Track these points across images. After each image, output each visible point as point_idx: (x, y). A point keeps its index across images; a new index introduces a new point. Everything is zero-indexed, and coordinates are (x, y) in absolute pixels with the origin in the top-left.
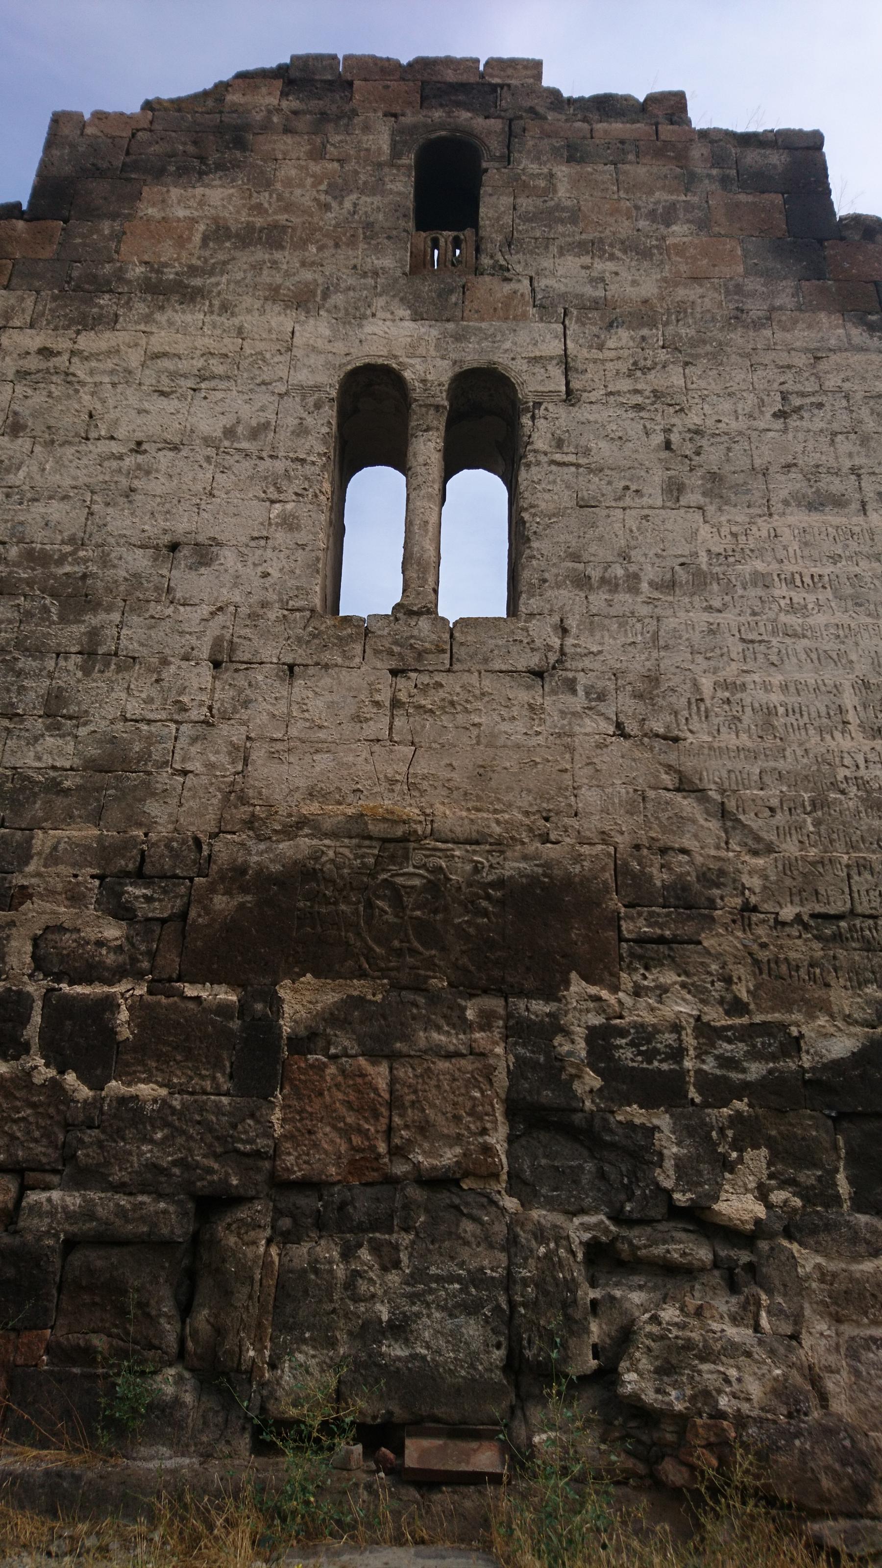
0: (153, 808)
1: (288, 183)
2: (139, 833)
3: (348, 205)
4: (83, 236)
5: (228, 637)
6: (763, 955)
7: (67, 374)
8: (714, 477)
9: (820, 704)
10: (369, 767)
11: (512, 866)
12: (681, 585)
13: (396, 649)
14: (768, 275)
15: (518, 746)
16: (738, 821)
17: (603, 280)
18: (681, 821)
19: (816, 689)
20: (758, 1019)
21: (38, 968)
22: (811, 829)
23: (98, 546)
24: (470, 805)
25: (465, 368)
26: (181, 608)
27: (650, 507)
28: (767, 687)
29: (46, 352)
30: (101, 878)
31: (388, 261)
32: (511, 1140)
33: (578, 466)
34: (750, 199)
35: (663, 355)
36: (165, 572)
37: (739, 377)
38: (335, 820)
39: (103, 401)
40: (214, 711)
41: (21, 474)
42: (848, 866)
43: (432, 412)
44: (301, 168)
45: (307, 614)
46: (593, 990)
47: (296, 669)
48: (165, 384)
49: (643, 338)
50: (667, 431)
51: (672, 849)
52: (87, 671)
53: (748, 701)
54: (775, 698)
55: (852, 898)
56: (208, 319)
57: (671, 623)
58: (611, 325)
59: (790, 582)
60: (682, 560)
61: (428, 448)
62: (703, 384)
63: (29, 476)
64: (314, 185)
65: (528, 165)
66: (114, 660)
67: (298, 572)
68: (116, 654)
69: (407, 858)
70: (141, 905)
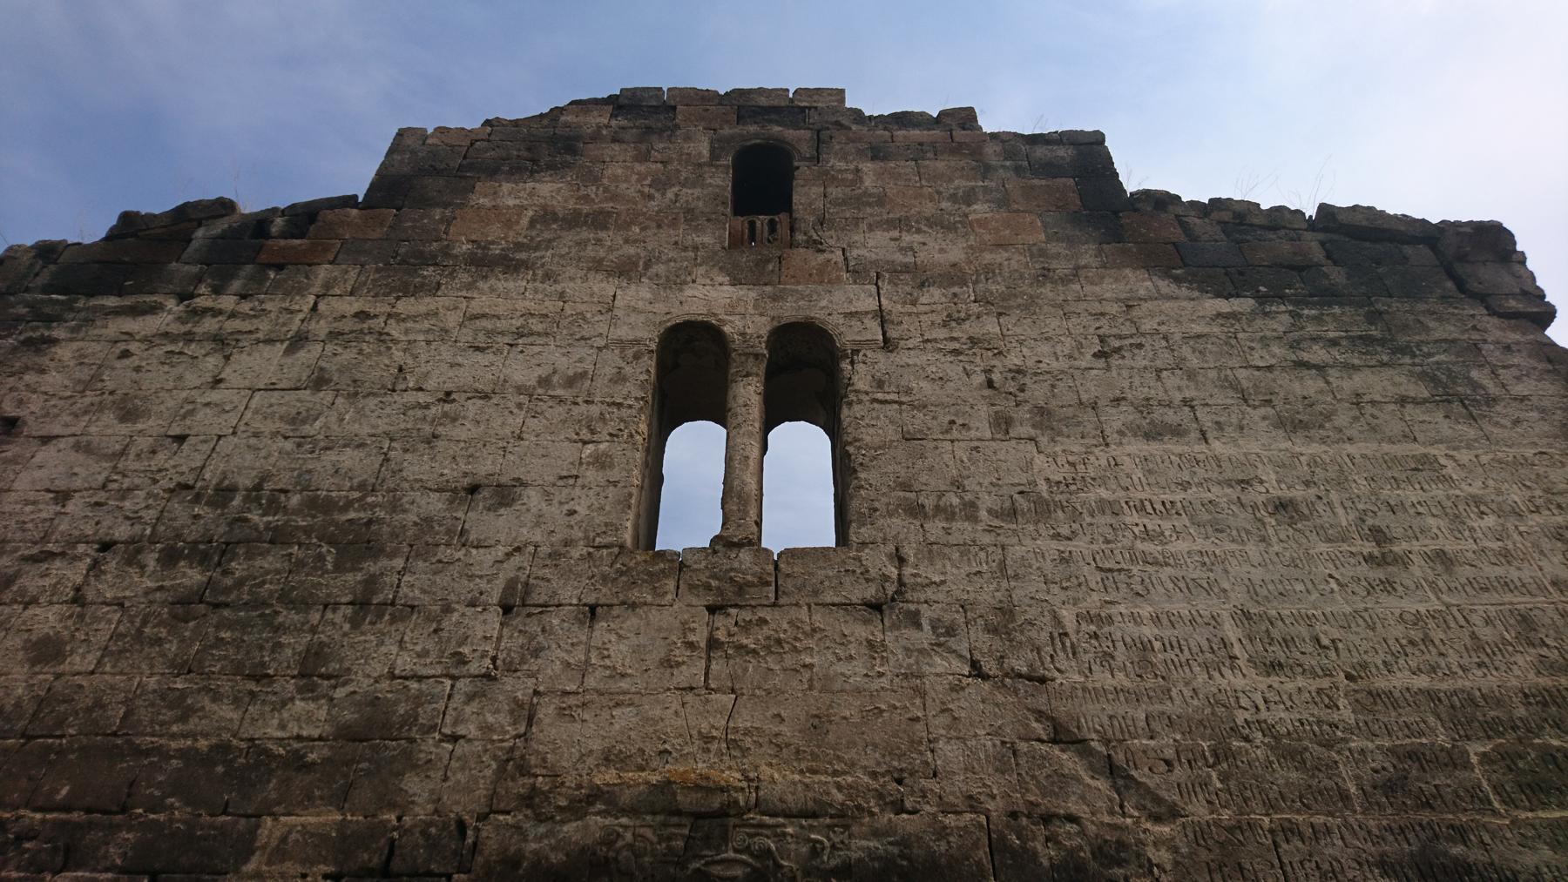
0: (413, 784)
1: (615, 178)
3: (670, 194)
4: (414, 220)
5: (523, 578)
7: (381, 334)
9: (1199, 637)
10: (680, 722)
11: (861, 846)
12: (1023, 514)
13: (714, 583)
14: (1071, 241)
15: (858, 691)
16: (1132, 778)
17: (912, 249)
18: (1062, 780)
19: (1192, 621)
22: (1219, 785)
23: (389, 491)
24: (803, 766)
26: (474, 551)
27: (979, 440)
28: (1136, 619)
29: (362, 315)
33: (900, 403)
34: (1043, 182)
35: (975, 308)
36: (460, 514)
37: (1054, 324)
38: (635, 791)
39: (415, 357)
40: (499, 662)
41: (318, 424)
42: (1272, 831)
43: (751, 359)
45: (616, 550)
47: (599, 610)
48: (481, 340)
49: (955, 295)
50: (988, 371)
51: (1057, 816)
52: (355, 623)
53: (1118, 635)
54: (1148, 631)
55: (1285, 873)
56: (530, 286)
57: (1017, 552)
58: (922, 285)
59: (1140, 508)
60: (1021, 488)
61: (748, 394)
62: (1019, 330)
63: (326, 426)
64: (638, 181)
66: (390, 609)
67: (607, 508)
68: (393, 604)
69: (725, 838)
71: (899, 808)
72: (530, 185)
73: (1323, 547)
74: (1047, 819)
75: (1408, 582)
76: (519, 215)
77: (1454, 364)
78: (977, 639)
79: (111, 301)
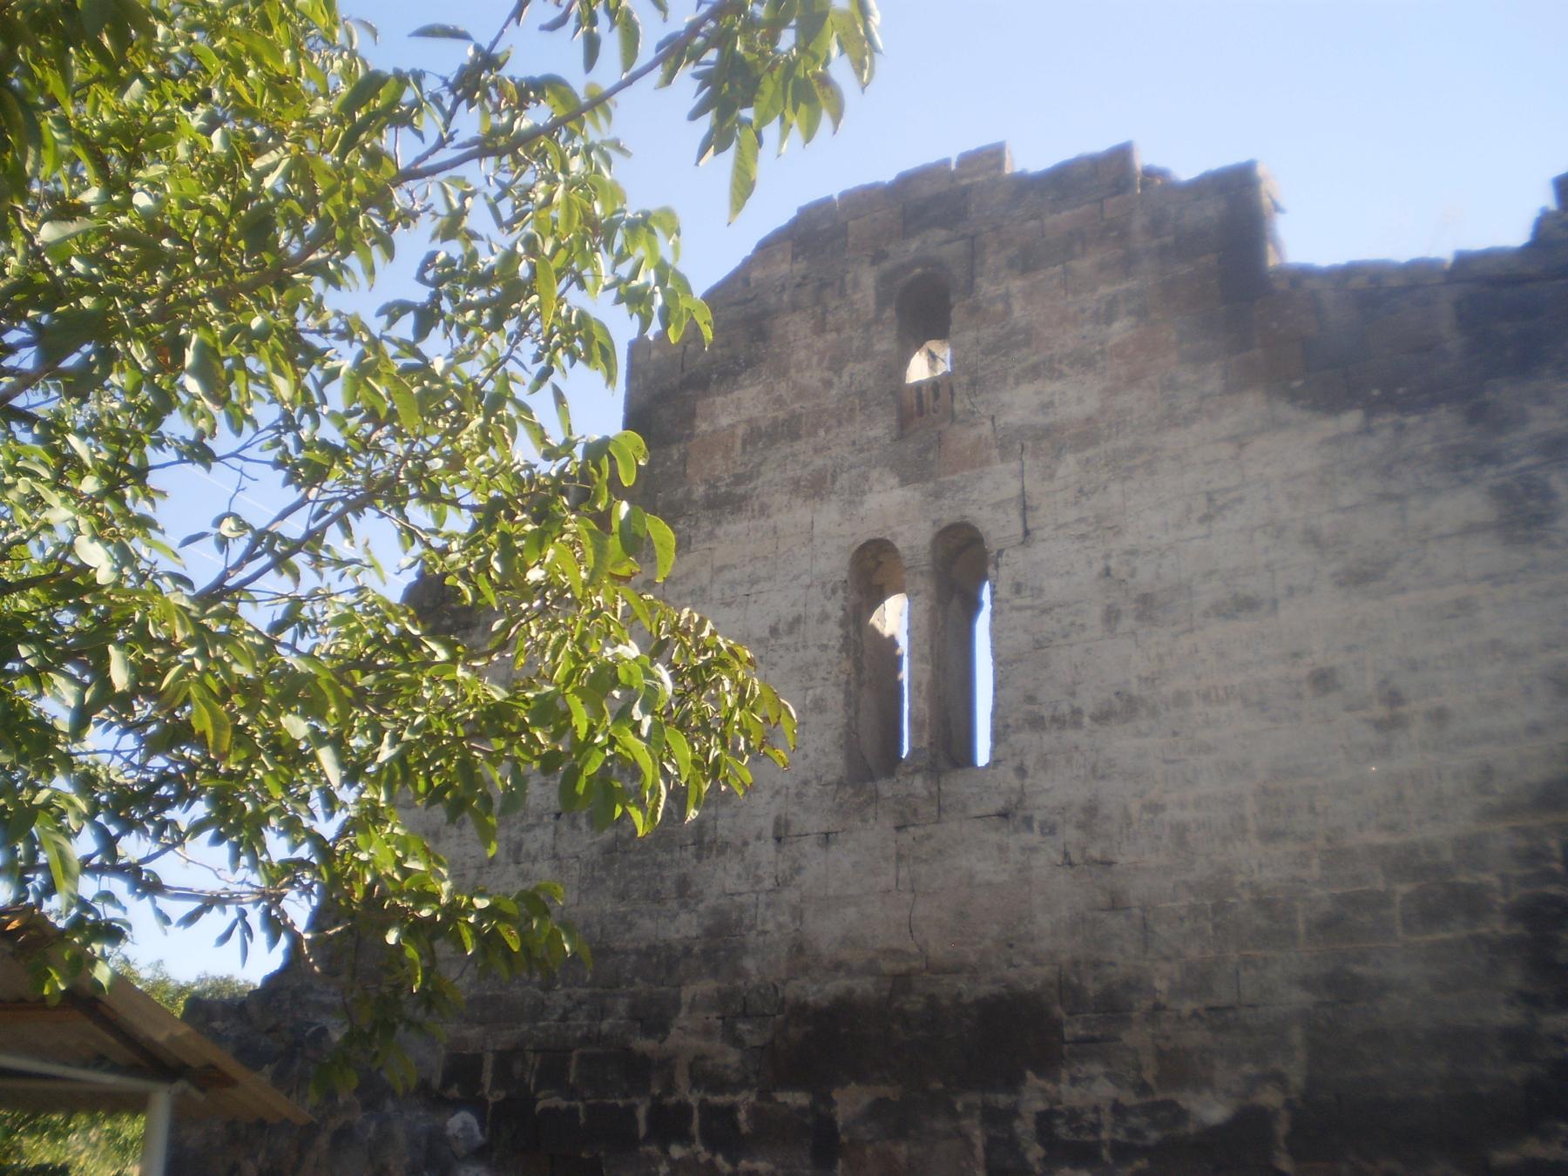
0: (749, 963)
2: (740, 983)
3: (846, 378)
8: (1146, 600)
11: (985, 989)
15: (989, 884)
20: (1160, 1096)
25: (944, 525)
28: (1183, 806)
30: (723, 1018)
31: (880, 429)
33: (1032, 608)
44: (808, 347)
46: (1041, 1083)
49: (1088, 460)
50: (1107, 556)
52: (699, 857)
59: (1206, 697)
65: (987, 288)
70: (747, 1037)
71: (1011, 965)
72: (736, 394)
74: (1097, 965)
76: (733, 435)
78: (1070, 834)
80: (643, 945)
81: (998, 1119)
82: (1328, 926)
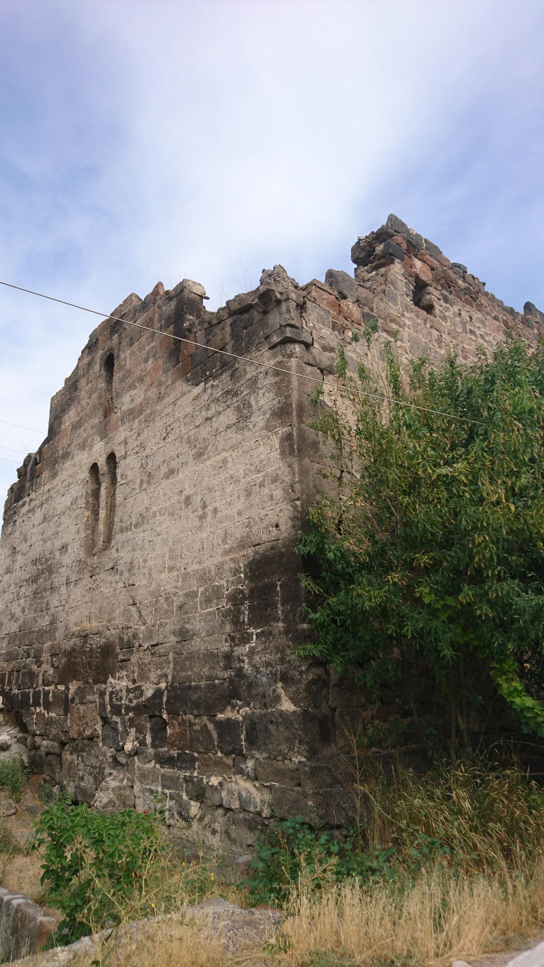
6: (140, 662)
14: (166, 371)
21: (43, 683)
29: (49, 490)
32: (103, 726)
65: (122, 356)
73: (192, 516)
74: (128, 628)
75: (205, 525)
77: (246, 395)
79: (20, 503)
80: (38, 629)
81: (102, 694)
82: (180, 608)
